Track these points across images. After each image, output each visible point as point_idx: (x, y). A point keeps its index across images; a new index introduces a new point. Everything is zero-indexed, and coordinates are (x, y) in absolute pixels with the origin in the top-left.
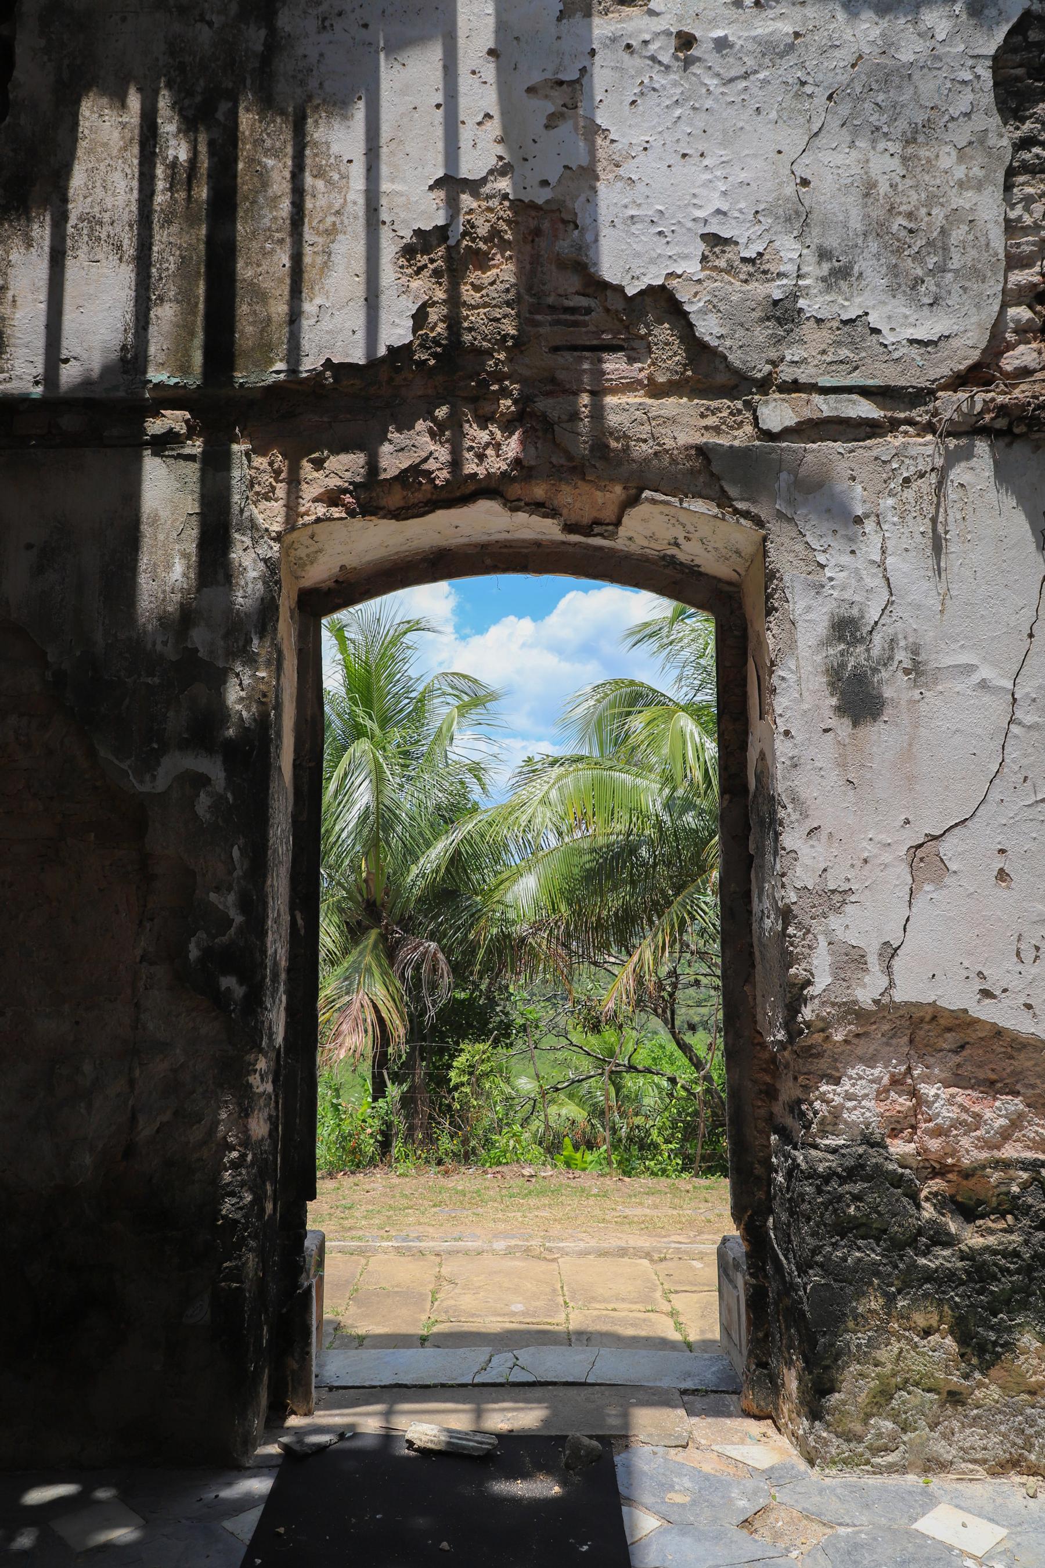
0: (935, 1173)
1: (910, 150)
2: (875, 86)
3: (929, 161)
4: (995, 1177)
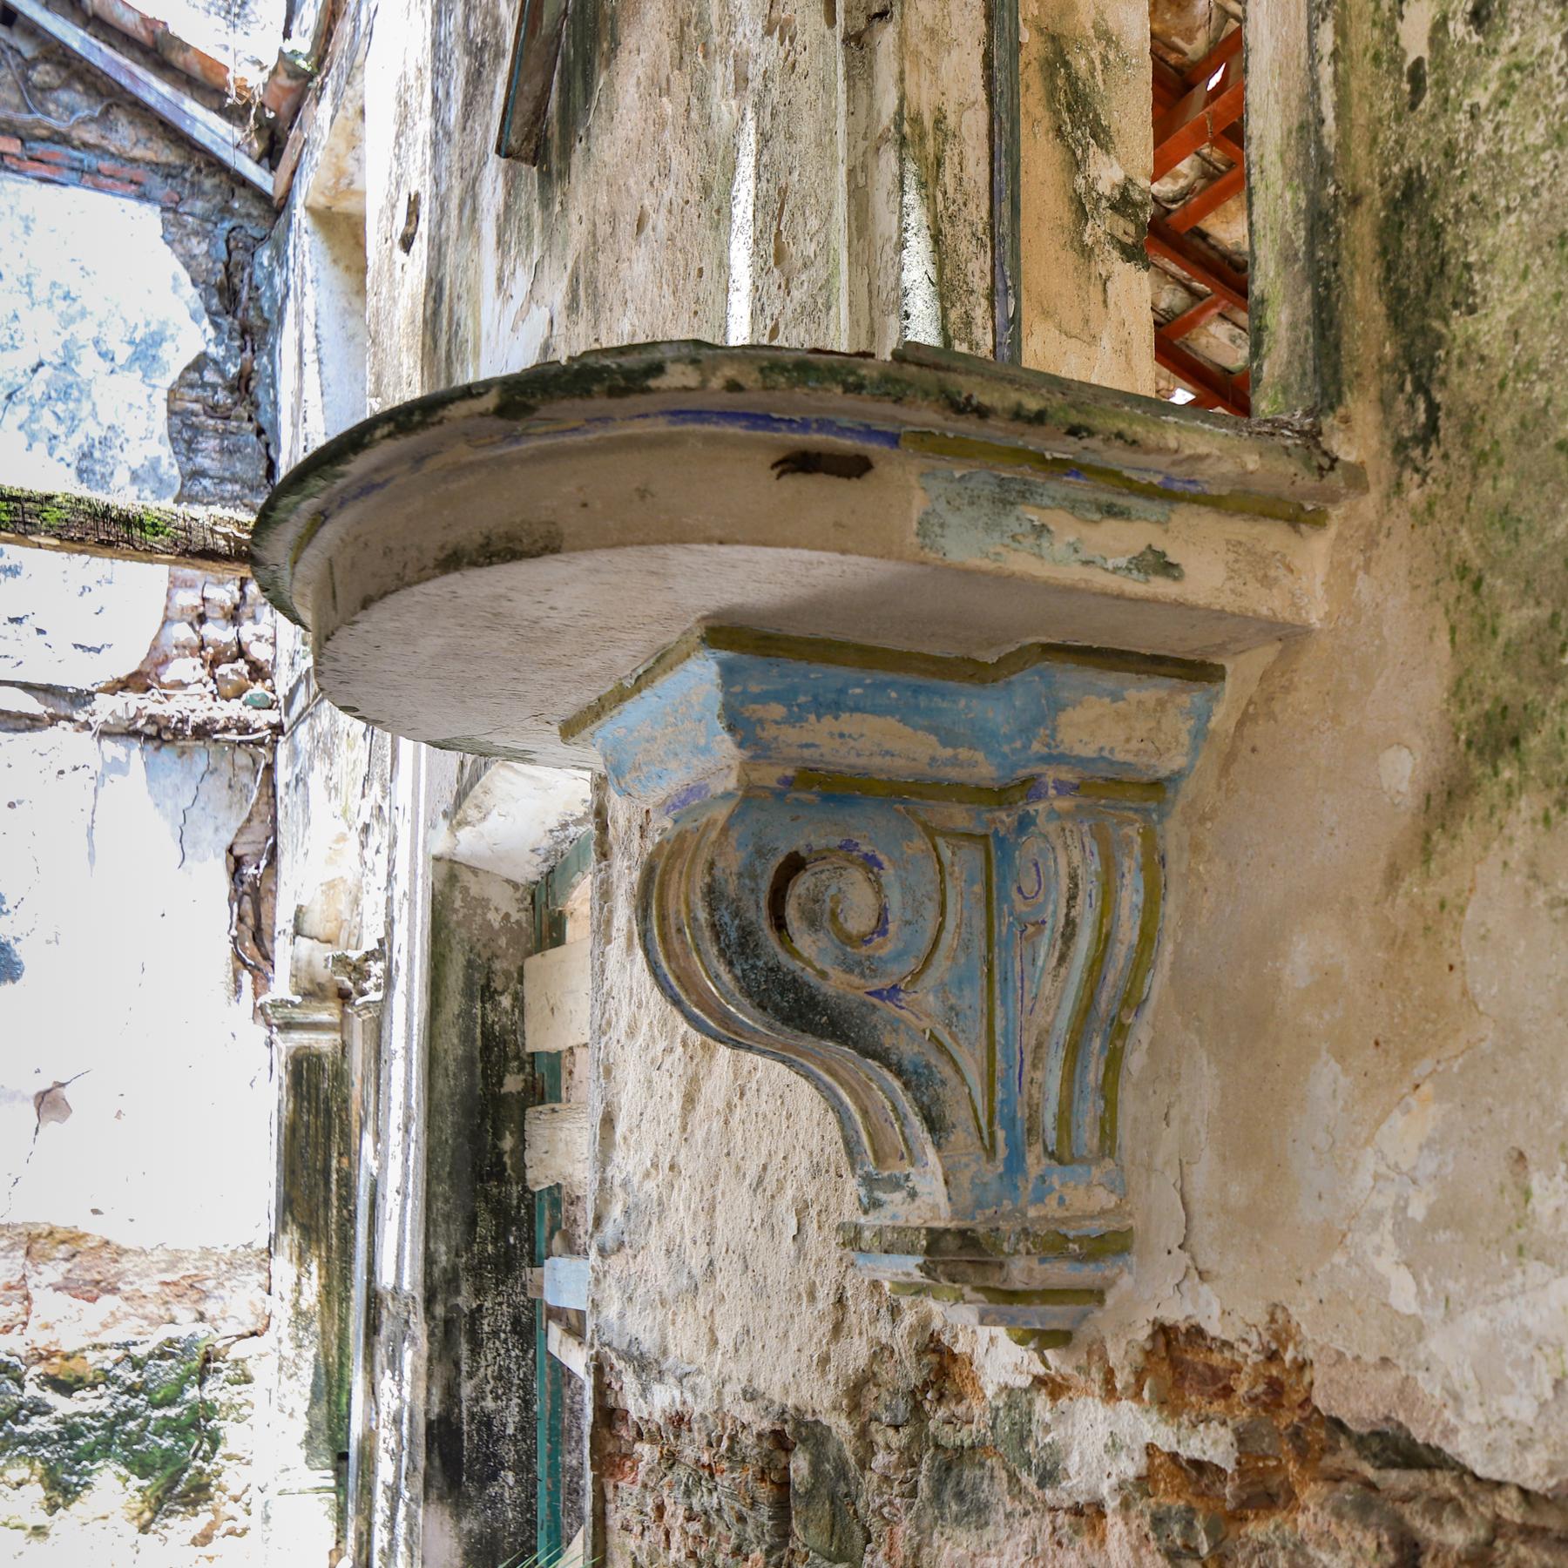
0: (41, 1358)
1: (85, 464)
2: (53, 394)
3: (103, 476)
4: (92, 1357)
